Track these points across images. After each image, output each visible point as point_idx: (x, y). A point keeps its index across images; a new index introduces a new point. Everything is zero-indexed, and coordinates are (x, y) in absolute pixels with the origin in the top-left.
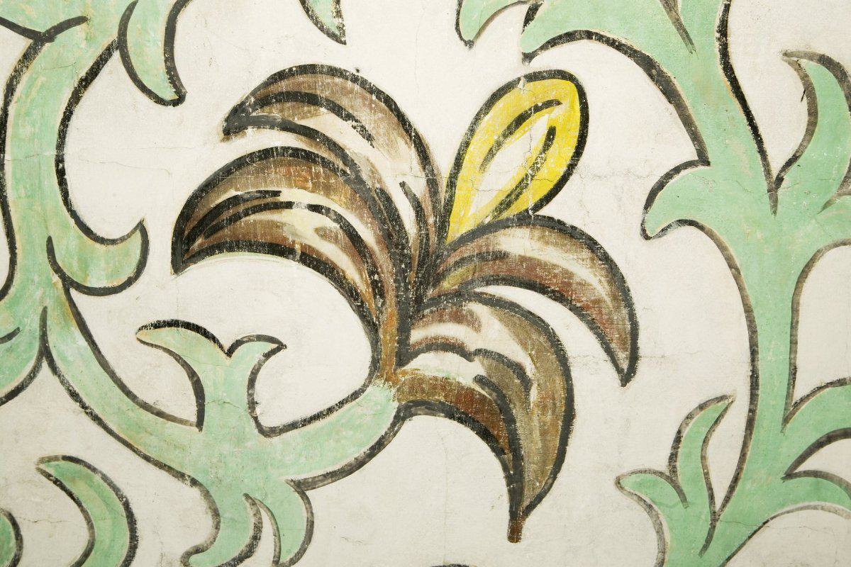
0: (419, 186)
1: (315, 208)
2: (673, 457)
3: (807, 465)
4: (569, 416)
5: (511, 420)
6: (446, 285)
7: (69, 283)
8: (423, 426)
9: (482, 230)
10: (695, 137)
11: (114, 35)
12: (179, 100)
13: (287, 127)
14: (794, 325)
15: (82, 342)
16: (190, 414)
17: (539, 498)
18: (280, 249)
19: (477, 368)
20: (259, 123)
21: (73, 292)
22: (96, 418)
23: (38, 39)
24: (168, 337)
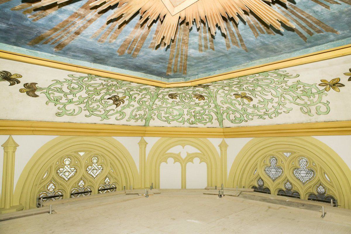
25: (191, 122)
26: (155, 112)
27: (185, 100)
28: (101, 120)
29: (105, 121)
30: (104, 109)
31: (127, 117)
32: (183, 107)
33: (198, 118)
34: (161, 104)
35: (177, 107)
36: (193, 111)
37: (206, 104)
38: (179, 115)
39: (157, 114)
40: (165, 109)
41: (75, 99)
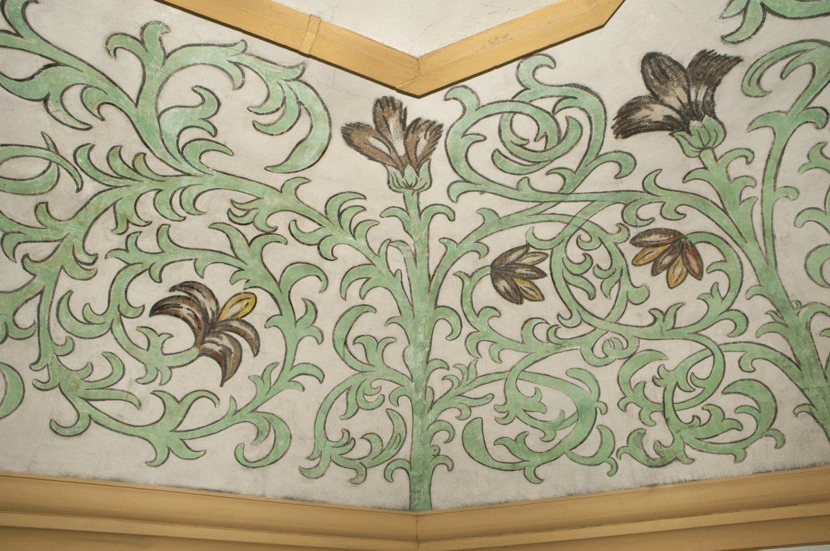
0: (214, 309)
2: (263, 374)
3: (294, 379)
4: (240, 361)
5: (226, 360)
6: (217, 330)
7: (121, 314)
8: (204, 358)
9: (227, 320)
10: (280, 310)
11: (148, 267)
12: (161, 282)
13: (185, 292)
14: (296, 350)
15: (121, 328)
16: (146, 347)
17: (229, 378)
18: (177, 316)
19: (220, 348)
20: (179, 290)
21: (122, 317)
22: (121, 345)
23: (129, 265)
24: (144, 330)
25: (653, 454)
26: (450, 416)
27: (591, 297)
28: (150, 464)
29: (176, 471)
30: (155, 386)
31: (299, 451)
32: (591, 358)
33: (686, 416)
34: (466, 359)
35: (557, 365)
36: (647, 373)
37: (718, 306)
38: (579, 412)
39: (459, 426)
40: (497, 388)
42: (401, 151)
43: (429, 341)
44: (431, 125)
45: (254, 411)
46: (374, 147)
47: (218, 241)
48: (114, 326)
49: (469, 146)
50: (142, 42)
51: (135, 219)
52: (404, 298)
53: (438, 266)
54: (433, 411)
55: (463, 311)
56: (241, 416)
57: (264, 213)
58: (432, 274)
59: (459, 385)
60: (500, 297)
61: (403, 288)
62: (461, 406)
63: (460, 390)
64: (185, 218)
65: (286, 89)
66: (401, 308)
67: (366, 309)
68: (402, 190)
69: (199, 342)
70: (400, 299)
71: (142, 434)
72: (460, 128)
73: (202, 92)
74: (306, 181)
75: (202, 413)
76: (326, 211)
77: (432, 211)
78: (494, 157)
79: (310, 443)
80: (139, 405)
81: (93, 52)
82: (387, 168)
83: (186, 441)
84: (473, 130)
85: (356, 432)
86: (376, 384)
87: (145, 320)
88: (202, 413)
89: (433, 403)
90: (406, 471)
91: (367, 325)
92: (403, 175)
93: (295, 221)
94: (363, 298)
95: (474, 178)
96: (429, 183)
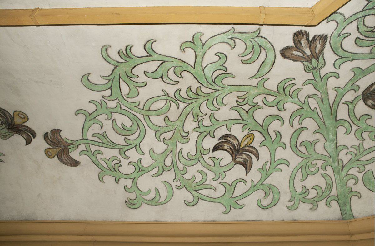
0: (237, 144)
1: (227, 146)
2: (263, 167)
3: (276, 167)
4: (252, 164)
5: (246, 164)
7: (202, 154)
8: (237, 165)
9: (244, 147)
10: (265, 138)
11: (208, 132)
12: (214, 137)
18: (223, 150)
19: (243, 160)
20: (222, 139)
22: (204, 166)
23: (201, 133)
24: (211, 158)
26: (354, 171)
28: (224, 213)
29: (235, 215)
30: (220, 180)
31: (285, 198)
34: (357, 143)
39: (360, 176)
41: (147, 161)
42: (308, 52)
43: (335, 138)
44: (322, 37)
45: (262, 184)
46: (296, 55)
47: (235, 115)
48: (200, 159)
49: (342, 41)
50: (193, 43)
51: (201, 114)
52: (320, 120)
53: (334, 101)
54: (344, 170)
55: (351, 120)
56: (257, 188)
57: (251, 98)
58: (331, 106)
59: (355, 156)
60: (370, 109)
61: (319, 115)
62: (359, 166)
63: (357, 158)
64: (220, 109)
65: (253, 42)
66: (319, 125)
67: (303, 129)
68: (311, 71)
69: (234, 159)
70: (318, 121)
71: (219, 201)
72: (336, 33)
73: (219, 54)
74: (267, 79)
75: (241, 189)
76: (278, 90)
77: (328, 76)
78: (356, 42)
79: (289, 194)
80: (215, 190)
81: (176, 53)
82: (303, 63)
83: (237, 201)
84: (343, 32)
85: (309, 186)
86: (314, 162)
87: (211, 154)
88: (241, 189)
89: (343, 166)
90: (337, 201)
91: (305, 136)
92: (311, 64)
93: (265, 98)
94: (300, 124)
95: (347, 55)
96: (324, 64)
